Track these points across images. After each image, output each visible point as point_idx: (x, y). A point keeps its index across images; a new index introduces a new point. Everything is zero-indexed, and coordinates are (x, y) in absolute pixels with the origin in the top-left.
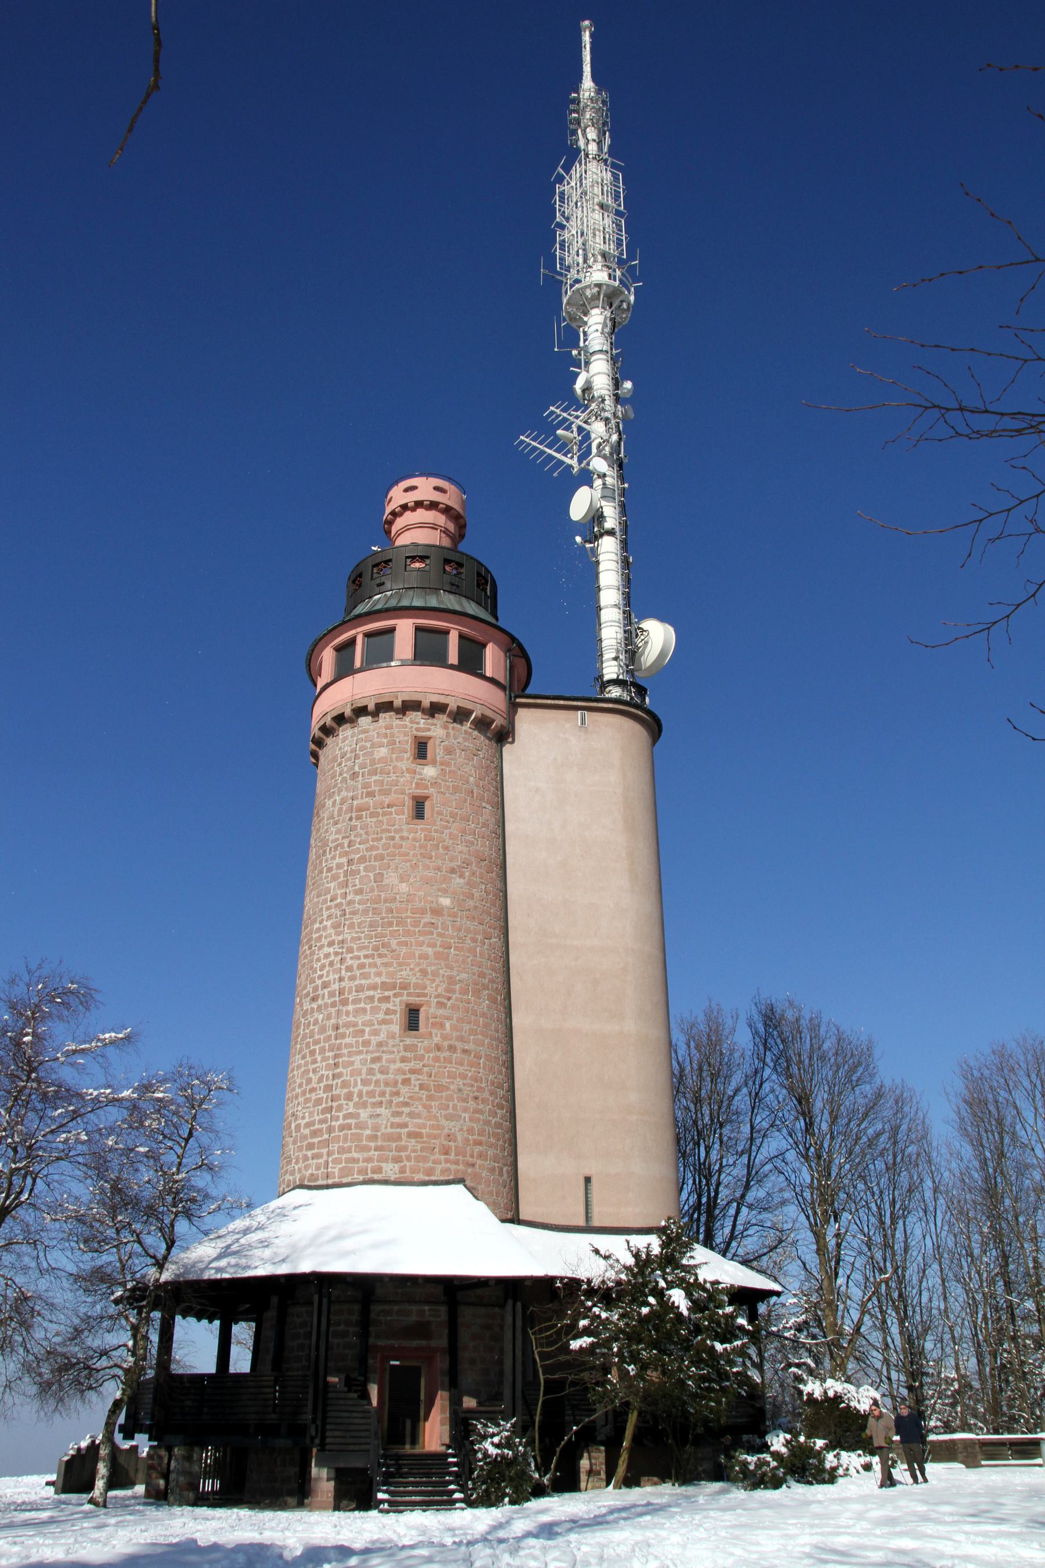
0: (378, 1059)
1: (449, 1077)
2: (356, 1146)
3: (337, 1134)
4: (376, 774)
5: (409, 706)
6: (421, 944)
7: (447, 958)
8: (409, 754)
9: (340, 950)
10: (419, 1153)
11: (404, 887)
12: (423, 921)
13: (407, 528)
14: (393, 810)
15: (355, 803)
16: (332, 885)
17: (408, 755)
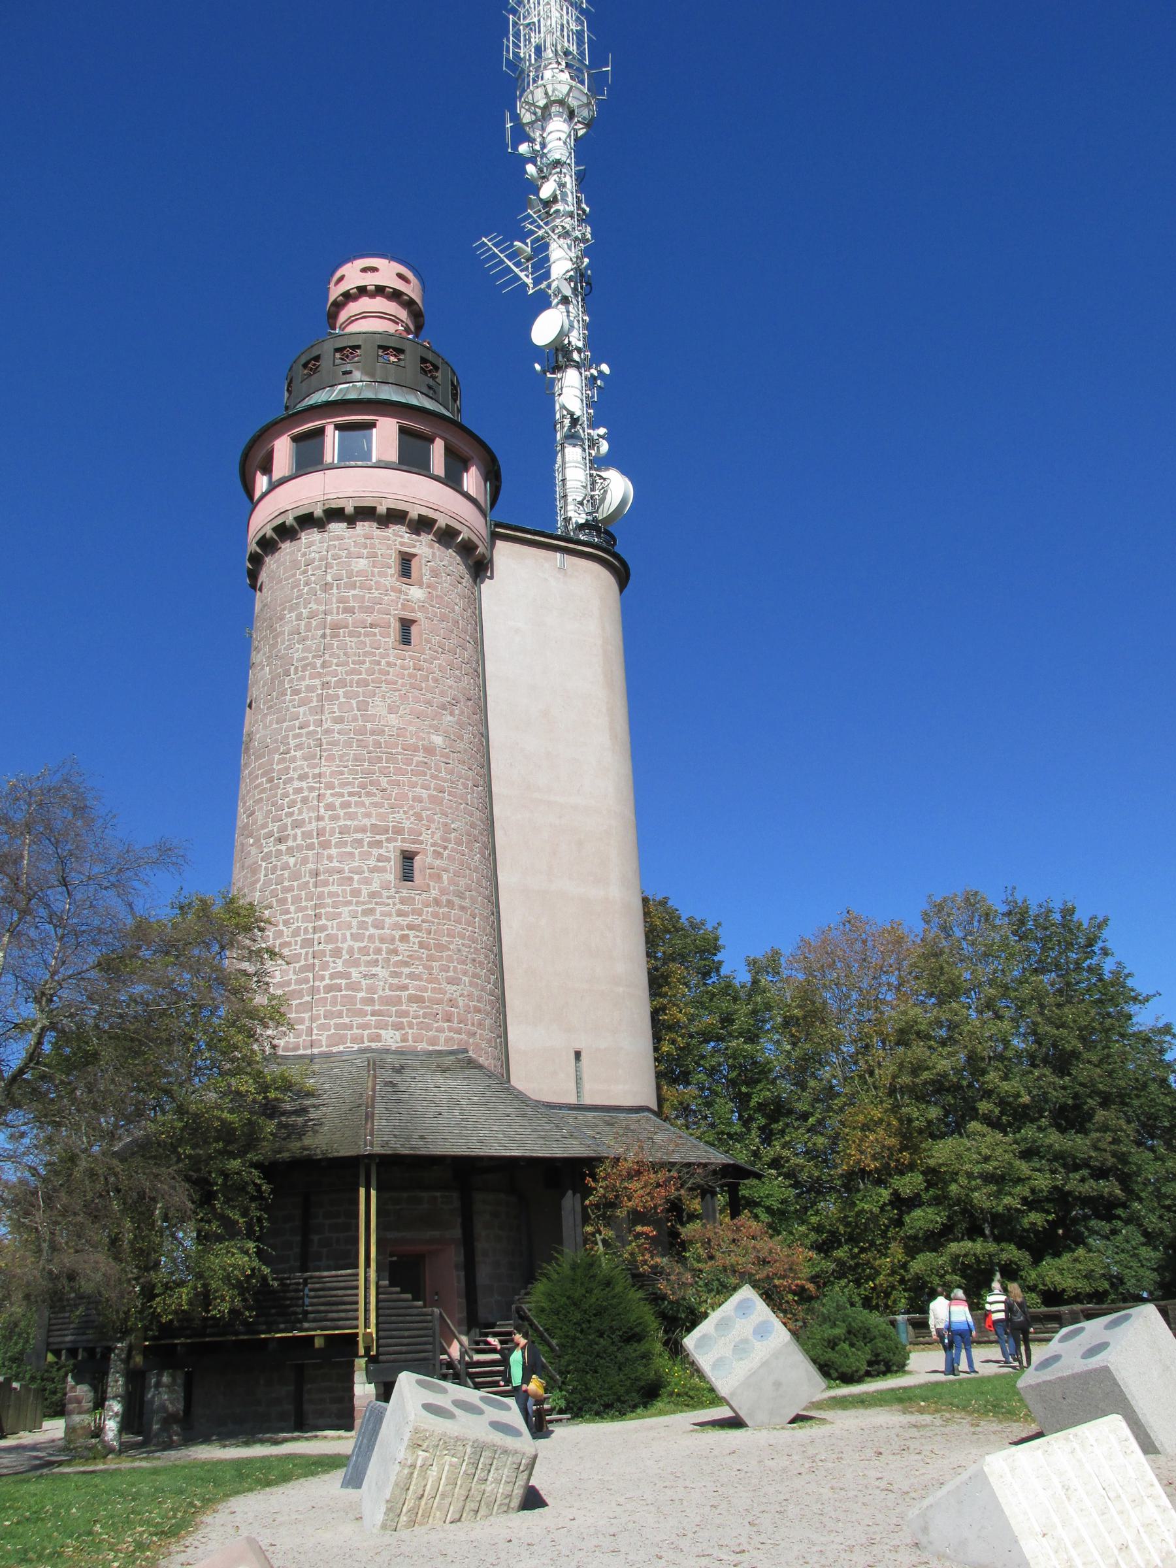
0: (371, 911)
1: (448, 935)
2: (347, 1009)
3: (322, 995)
4: (355, 589)
5: (395, 517)
6: (414, 785)
7: (441, 804)
8: (393, 569)
9: (318, 785)
10: (422, 1020)
11: (393, 719)
12: (415, 759)
13: (364, 316)
14: (377, 630)
15: (329, 618)
16: (301, 710)
17: (391, 571)
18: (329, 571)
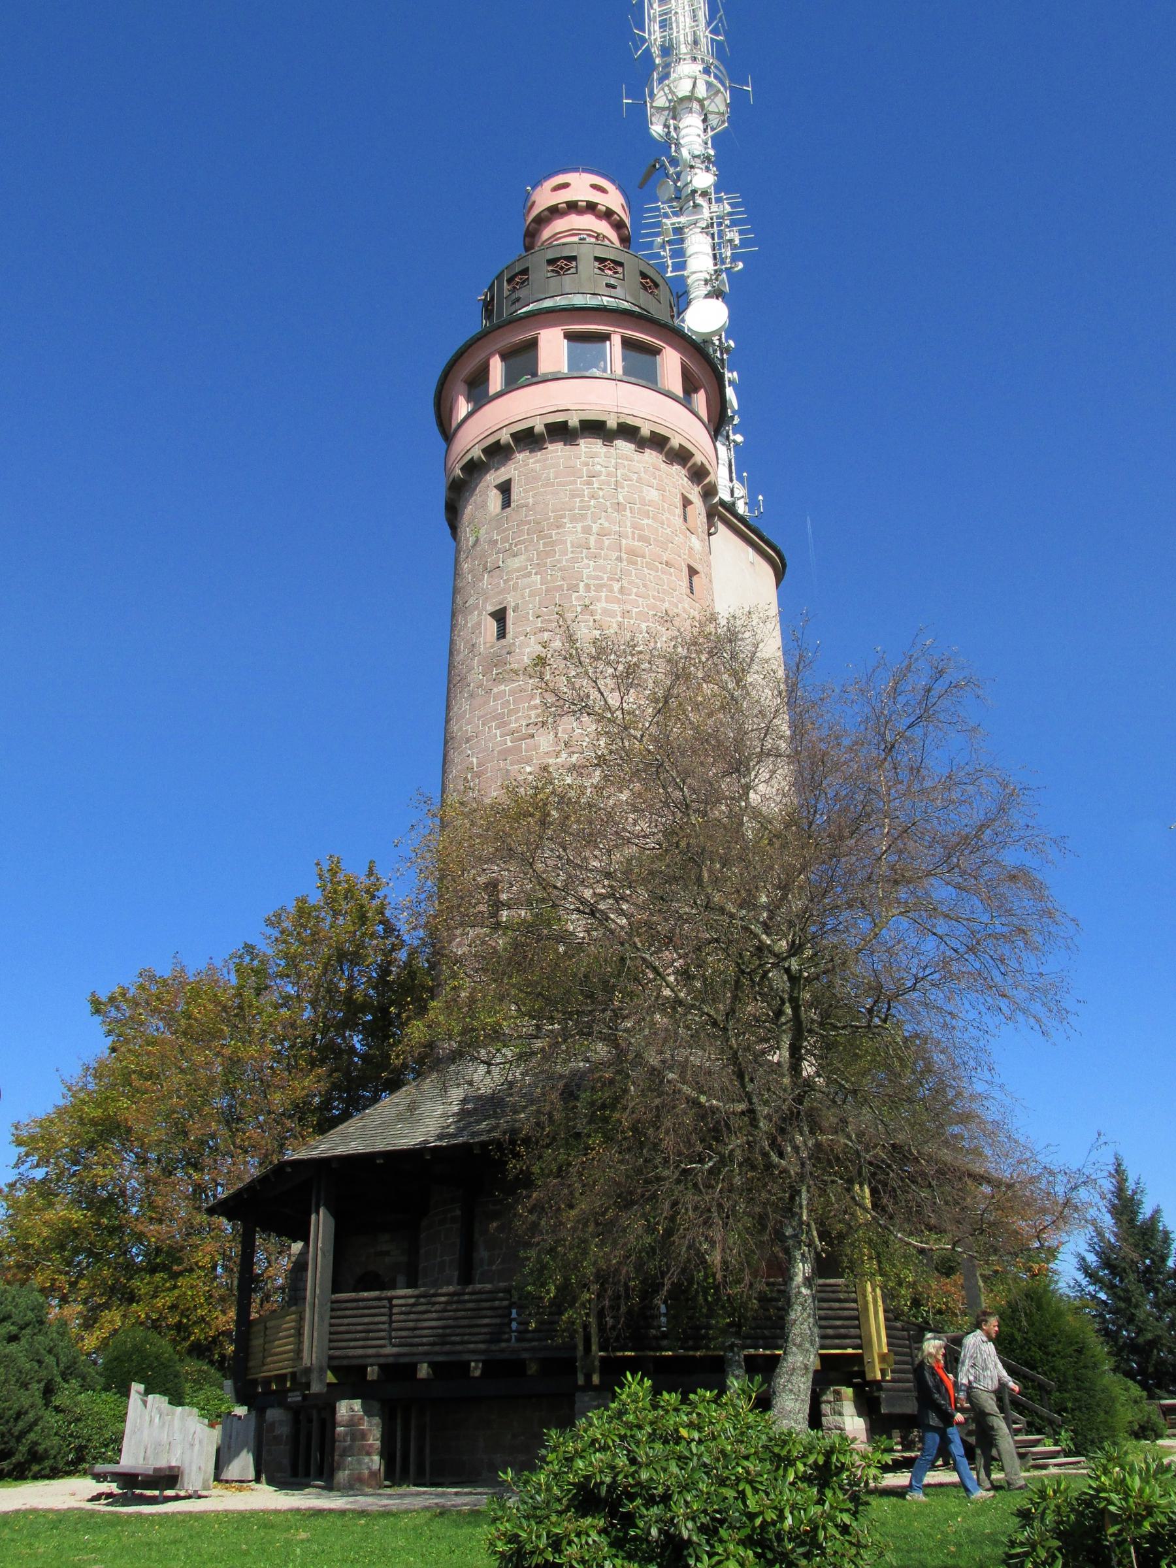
18: (619, 490)
